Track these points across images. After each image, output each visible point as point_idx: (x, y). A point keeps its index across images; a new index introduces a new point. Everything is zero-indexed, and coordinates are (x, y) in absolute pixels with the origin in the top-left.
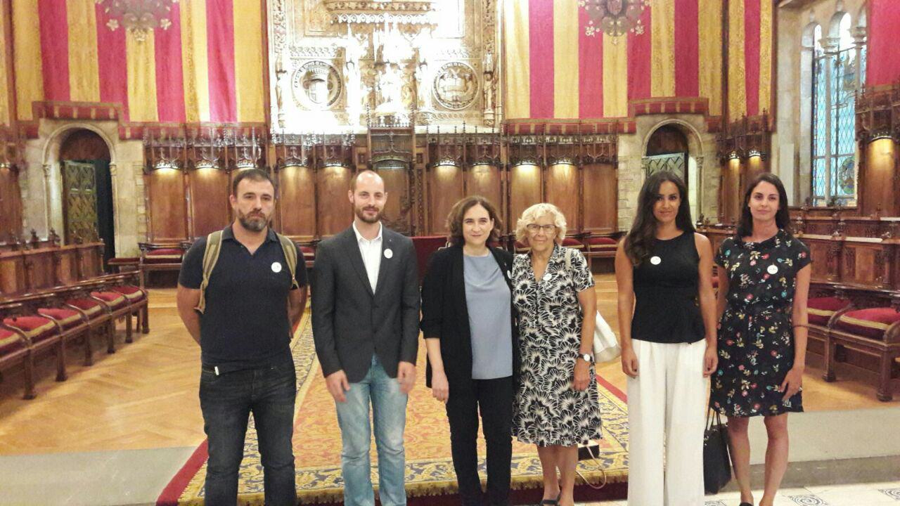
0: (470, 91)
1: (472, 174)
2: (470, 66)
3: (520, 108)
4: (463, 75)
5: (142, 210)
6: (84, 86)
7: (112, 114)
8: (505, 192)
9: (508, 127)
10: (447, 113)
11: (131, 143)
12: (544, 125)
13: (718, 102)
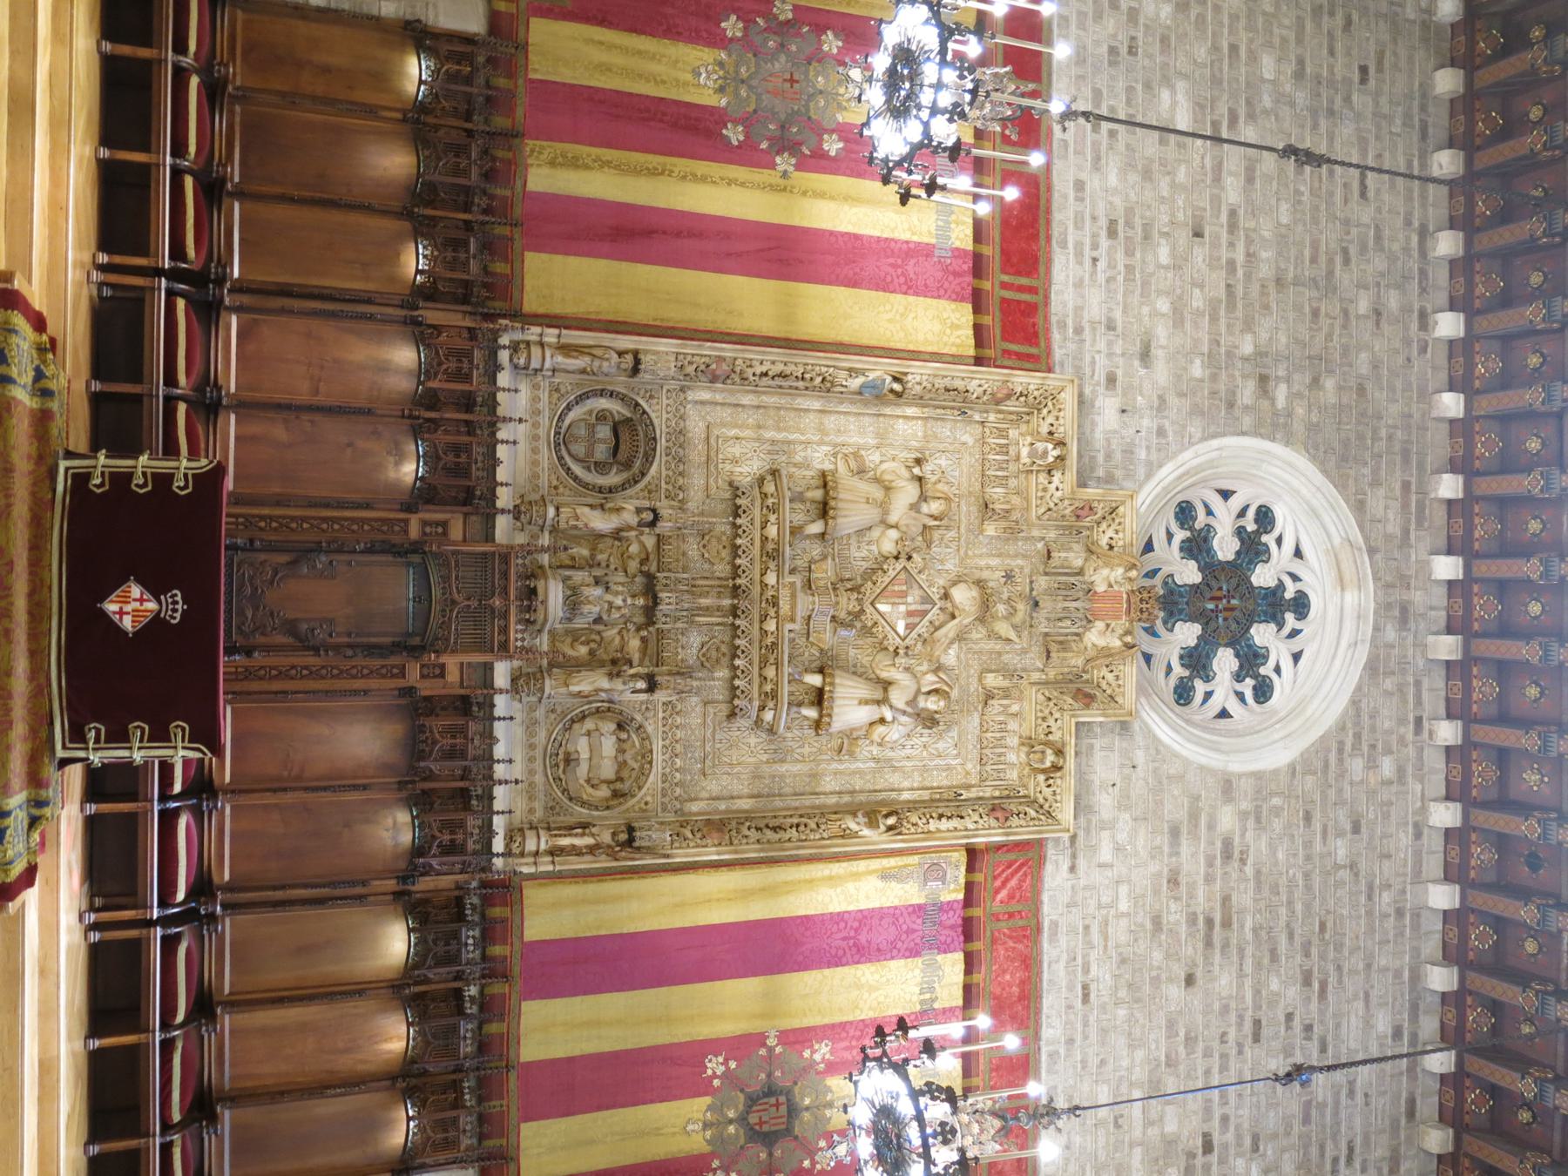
0: (589, 793)
2: (644, 790)
3: (547, 916)
4: (625, 774)
8: (338, 892)
10: (542, 736)
12: (505, 976)
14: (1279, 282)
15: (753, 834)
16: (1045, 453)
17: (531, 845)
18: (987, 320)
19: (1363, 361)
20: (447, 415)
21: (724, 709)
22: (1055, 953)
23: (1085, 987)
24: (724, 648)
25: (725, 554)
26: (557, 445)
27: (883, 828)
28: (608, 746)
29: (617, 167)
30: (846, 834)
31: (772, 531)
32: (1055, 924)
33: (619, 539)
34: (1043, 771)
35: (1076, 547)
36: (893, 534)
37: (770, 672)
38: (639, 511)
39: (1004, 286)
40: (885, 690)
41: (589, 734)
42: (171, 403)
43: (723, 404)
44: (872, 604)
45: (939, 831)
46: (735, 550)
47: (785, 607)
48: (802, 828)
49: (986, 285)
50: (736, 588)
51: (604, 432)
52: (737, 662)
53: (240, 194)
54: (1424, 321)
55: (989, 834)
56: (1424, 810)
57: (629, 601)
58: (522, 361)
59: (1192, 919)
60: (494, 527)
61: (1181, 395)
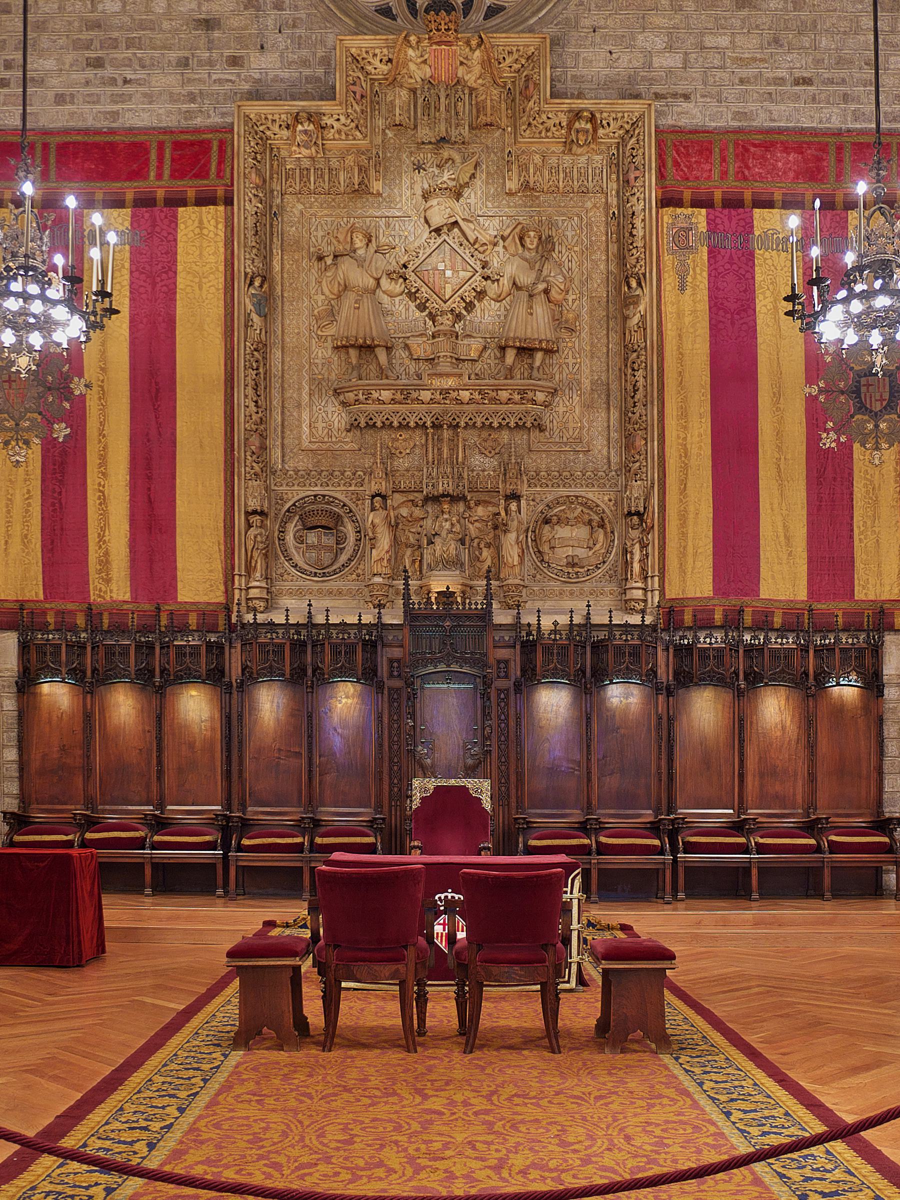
1: (602, 701)
3: (694, 577)
4: (586, 518)
9: (671, 614)
10: (555, 586)
15: (639, 409)
16: (306, 132)
17: (639, 594)
18: (191, 194)
20: (309, 659)
21: (535, 434)
22: (763, 115)
23: (797, 82)
24: (485, 434)
25: (405, 435)
26: (324, 575)
27: (639, 292)
28: (563, 532)
29: (103, 529)
30: (642, 326)
31: (386, 395)
32: (737, 115)
33: (397, 524)
34: (595, 130)
35: (389, 98)
36: (385, 283)
38: (373, 509)
39: (159, 176)
40: (519, 288)
41: (552, 548)
43: (283, 438)
44: (445, 302)
45: (644, 237)
47: (450, 382)
48: (636, 366)
49: (160, 194)
50: (434, 426)
51: (312, 538)
52: (495, 425)
53: (161, 806)
55: (648, 187)
57: (446, 516)
58: (262, 604)
60: (391, 625)
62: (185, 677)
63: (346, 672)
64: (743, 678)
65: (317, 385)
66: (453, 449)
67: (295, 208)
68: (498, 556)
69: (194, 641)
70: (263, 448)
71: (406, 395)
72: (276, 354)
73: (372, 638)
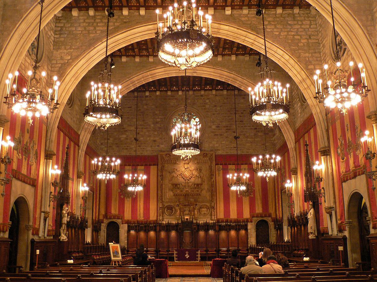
1: (209, 233)
3: (221, 215)
5: (126, 241)
6: (114, 211)
7: (120, 218)
11: (124, 224)
13: (275, 214)
14: (144, 121)
18: (152, 164)
19: (153, 107)
21: (199, 196)
28: (203, 209)
30: (213, 181)
37: (195, 191)
42: (169, 254)
46: (181, 195)
47: (188, 189)
51: (169, 211)
53: (147, 249)
54: (147, 97)
56: (213, 95)
59: (227, 132)
61: (159, 136)
62: (152, 230)
63: (173, 230)
64: (228, 228)
65: (169, 189)
66: (188, 199)
67: (166, 165)
68: (194, 214)
69: (152, 225)
70: (162, 198)
71: (181, 191)
72: (164, 185)
73: (177, 225)
